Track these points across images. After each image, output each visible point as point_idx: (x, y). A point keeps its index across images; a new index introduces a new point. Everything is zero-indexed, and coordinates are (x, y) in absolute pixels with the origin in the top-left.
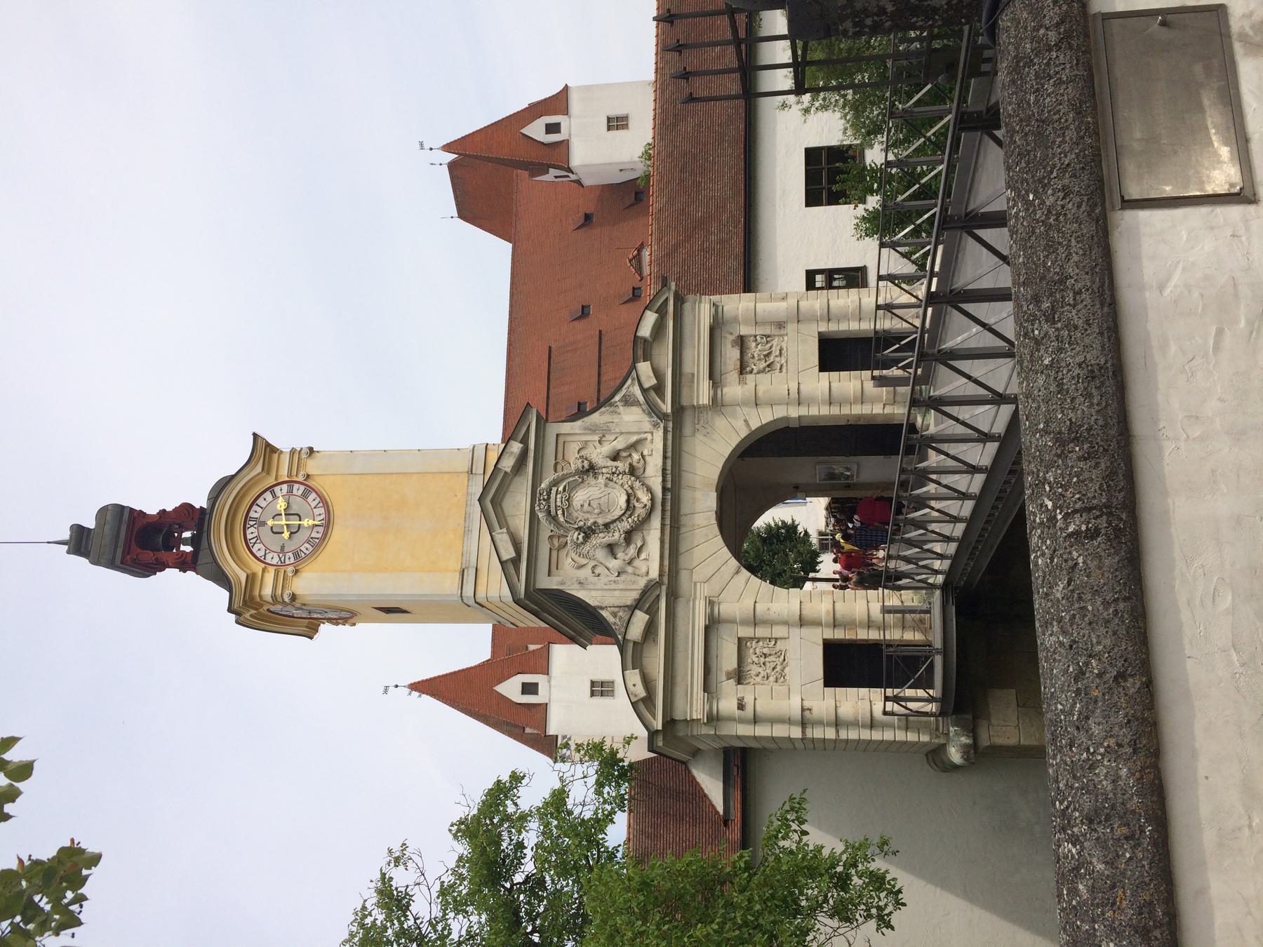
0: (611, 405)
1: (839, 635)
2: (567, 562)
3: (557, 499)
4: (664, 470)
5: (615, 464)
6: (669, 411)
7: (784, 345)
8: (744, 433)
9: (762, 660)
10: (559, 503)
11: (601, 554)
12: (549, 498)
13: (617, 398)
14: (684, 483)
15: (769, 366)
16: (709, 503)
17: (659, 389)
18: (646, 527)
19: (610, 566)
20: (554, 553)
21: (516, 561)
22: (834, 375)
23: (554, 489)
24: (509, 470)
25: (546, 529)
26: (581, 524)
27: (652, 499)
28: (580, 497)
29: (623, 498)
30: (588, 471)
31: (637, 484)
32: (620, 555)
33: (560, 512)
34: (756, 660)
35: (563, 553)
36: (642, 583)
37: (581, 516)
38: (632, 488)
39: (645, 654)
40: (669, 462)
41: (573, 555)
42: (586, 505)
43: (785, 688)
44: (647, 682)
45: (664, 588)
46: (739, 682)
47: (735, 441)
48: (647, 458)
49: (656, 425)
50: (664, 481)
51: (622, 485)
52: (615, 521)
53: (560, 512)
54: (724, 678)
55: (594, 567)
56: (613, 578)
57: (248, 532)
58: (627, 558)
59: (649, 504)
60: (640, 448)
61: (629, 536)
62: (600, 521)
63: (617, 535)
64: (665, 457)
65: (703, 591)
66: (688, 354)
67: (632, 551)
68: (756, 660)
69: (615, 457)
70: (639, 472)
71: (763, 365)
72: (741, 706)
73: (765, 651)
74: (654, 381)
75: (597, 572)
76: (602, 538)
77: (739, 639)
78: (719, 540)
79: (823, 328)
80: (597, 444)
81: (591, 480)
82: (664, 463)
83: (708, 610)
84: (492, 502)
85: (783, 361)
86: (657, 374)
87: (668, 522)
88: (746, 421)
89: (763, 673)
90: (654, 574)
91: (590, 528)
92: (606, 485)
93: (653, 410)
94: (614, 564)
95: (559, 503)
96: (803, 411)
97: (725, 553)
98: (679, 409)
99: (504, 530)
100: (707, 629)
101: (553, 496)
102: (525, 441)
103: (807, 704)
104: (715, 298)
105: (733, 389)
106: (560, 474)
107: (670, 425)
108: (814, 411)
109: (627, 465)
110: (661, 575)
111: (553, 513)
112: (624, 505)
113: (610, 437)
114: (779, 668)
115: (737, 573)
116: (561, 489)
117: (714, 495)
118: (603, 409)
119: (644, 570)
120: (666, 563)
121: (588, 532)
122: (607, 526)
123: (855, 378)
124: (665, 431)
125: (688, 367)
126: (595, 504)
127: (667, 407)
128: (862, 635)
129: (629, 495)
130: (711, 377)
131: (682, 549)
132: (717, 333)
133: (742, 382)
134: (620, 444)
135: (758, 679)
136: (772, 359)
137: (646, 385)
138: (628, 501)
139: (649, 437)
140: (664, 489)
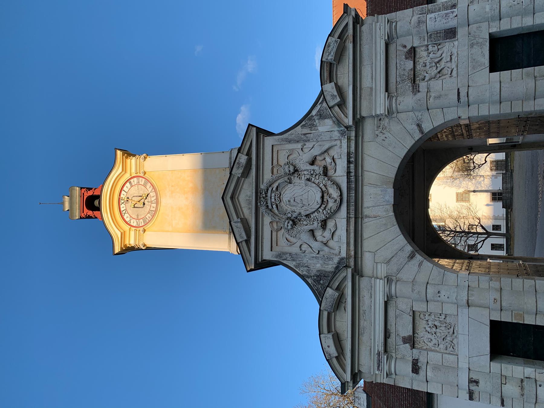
0: (310, 119)
1: (506, 318)
2: (282, 242)
3: (272, 197)
4: (349, 173)
5: (312, 167)
6: (351, 123)
7: (455, 51)
8: (418, 136)
9: (434, 329)
10: (273, 200)
11: (305, 237)
12: (266, 196)
13: (314, 113)
14: (366, 181)
15: (439, 72)
16: (387, 198)
17: (342, 105)
18: (338, 215)
19: (312, 246)
20: (274, 234)
21: (248, 242)
22: (506, 74)
23: (270, 189)
24: (239, 176)
25: (267, 219)
26: (289, 215)
27: (341, 195)
28: (288, 193)
29: (319, 195)
30: (293, 173)
31: (329, 183)
32: (319, 238)
33: (274, 206)
34: (428, 329)
35: (281, 233)
36: (336, 260)
37: (289, 209)
38: (325, 186)
39: (338, 318)
40: (352, 166)
41: (288, 236)
42: (292, 201)
43: (452, 358)
44: (338, 340)
45: (350, 270)
46: (413, 347)
47: (409, 143)
48: (338, 161)
49: (342, 134)
50: (349, 182)
51: (318, 185)
52: (314, 212)
53: (274, 206)
54: (400, 342)
55: (300, 247)
56: (315, 255)
57: (121, 206)
58: (325, 240)
59: (338, 200)
60: (332, 152)
61: (324, 224)
62: (304, 213)
63: (316, 223)
64: (349, 162)
65: (382, 270)
66: (366, 72)
67: (327, 234)
68: (428, 329)
69: (312, 163)
70: (331, 173)
71: (434, 71)
72: (416, 369)
73: (436, 323)
74: (338, 99)
75: (303, 249)
76: (304, 227)
77: (413, 311)
78: (396, 229)
79: (493, 30)
80: (300, 151)
81: (295, 180)
82: (348, 167)
83: (387, 289)
84: (232, 198)
85: (454, 65)
86: (340, 91)
87: (352, 216)
88: (419, 126)
89: (434, 341)
90: (344, 254)
91: (296, 218)
92: (306, 185)
93: (338, 122)
94: (316, 245)
95: (273, 200)
96: (473, 112)
97: (401, 240)
98: (359, 122)
99: (239, 220)
100: (386, 304)
101: (269, 194)
102: (249, 154)
103: (475, 377)
104: (388, 16)
105: (407, 100)
106: (274, 177)
107: (353, 134)
108: (484, 111)
109: (321, 169)
110: (348, 256)
111: (270, 207)
112: (320, 201)
113: (309, 145)
114: (449, 338)
115: (411, 257)
116: (274, 189)
117: (391, 192)
118: (303, 123)
119: (337, 252)
120: (352, 247)
121: (294, 222)
122: (308, 216)
123: (528, 75)
124: (349, 139)
125: (366, 82)
126: (298, 200)
127: (349, 121)
128: (529, 320)
129: (323, 192)
130: (387, 90)
131: (365, 236)
132: (392, 48)
133: (415, 89)
134: (316, 151)
135: (430, 344)
136: (442, 64)
137: (331, 104)
138: (322, 197)
139: (338, 142)
140: (349, 188)
